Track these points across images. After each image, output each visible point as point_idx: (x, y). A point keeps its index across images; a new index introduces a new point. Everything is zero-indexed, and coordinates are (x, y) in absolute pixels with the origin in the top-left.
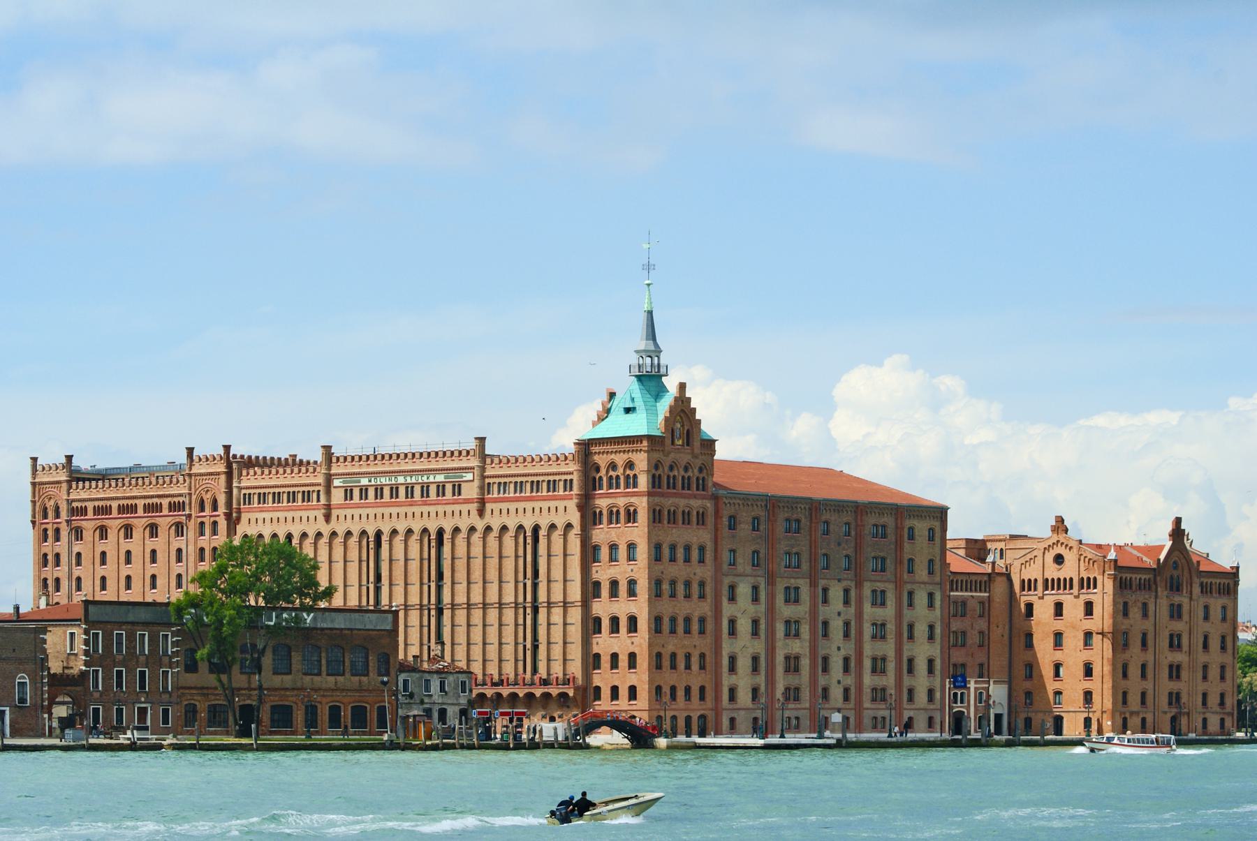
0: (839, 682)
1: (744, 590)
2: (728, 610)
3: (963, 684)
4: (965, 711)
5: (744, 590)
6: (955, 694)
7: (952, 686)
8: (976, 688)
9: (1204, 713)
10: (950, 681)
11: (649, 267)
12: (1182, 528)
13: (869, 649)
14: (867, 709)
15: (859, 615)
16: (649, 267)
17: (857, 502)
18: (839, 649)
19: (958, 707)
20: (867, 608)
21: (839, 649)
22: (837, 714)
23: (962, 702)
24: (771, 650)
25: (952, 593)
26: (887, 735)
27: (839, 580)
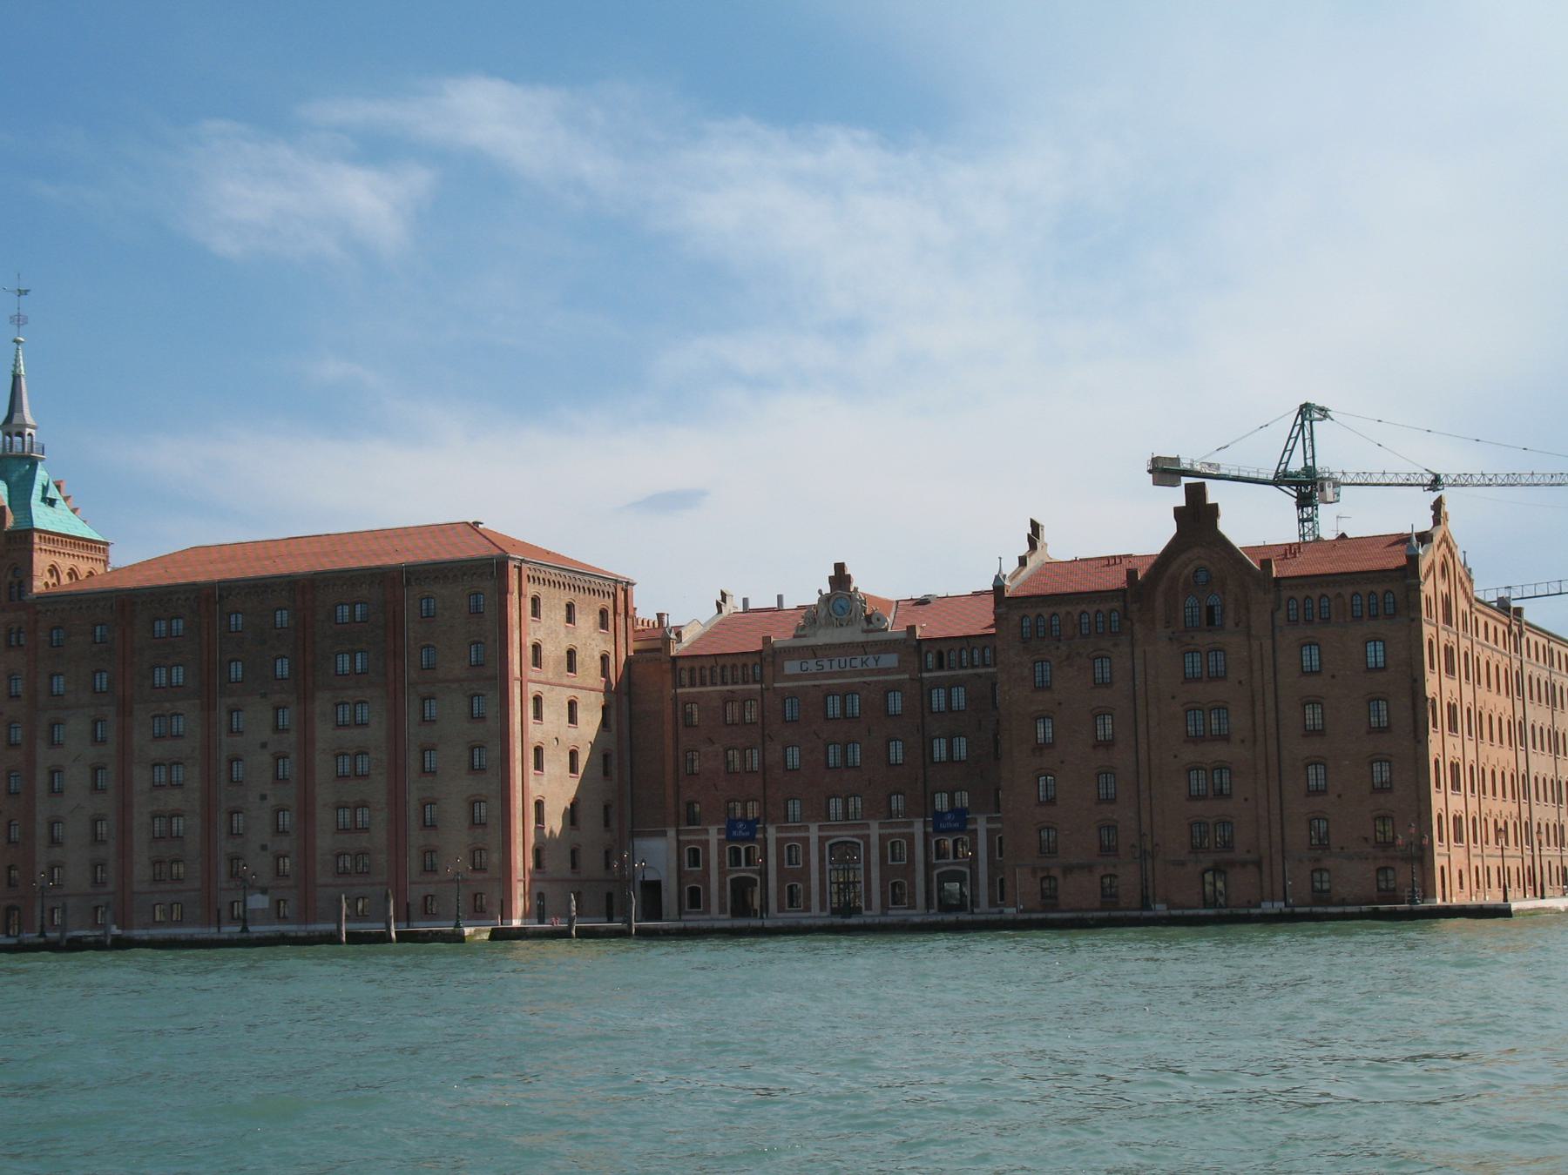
0: (264, 848)
1: (76, 728)
2: (45, 757)
3: (748, 834)
4: (968, 871)
5: (76, 728)
6: (737, 851)
7: (930, 830)
8: (988, 830)
9: (1318, 860)
10: (925, 822)
11: (19, 320)
12: (1210, 500)
13: (324, 793)
14: (326, 886)
15: (306, 743)
16: (19, 320)
17: (293, 576)
18: (263, 797)
19: (947, 864)
20: (324, 734)
21: (263, 797)
22: (259, 896)
23: (748, 863)
24: (125, 808)
25: (925, 675)
26: (238, 929)
27: (264, 696)
